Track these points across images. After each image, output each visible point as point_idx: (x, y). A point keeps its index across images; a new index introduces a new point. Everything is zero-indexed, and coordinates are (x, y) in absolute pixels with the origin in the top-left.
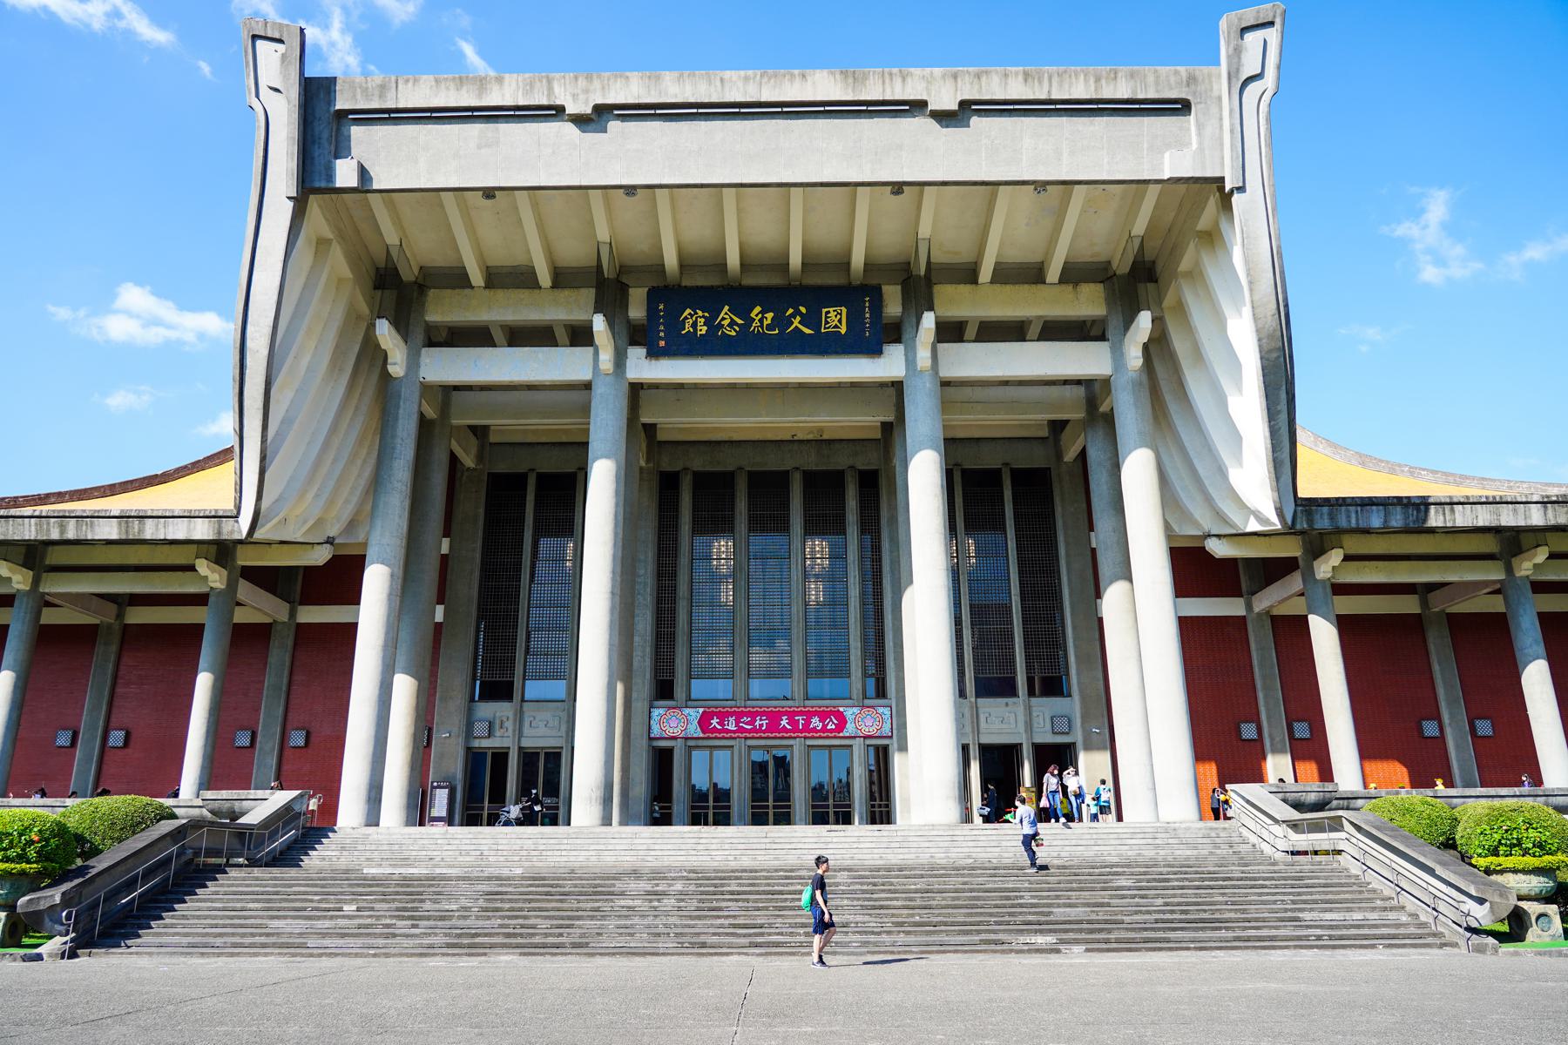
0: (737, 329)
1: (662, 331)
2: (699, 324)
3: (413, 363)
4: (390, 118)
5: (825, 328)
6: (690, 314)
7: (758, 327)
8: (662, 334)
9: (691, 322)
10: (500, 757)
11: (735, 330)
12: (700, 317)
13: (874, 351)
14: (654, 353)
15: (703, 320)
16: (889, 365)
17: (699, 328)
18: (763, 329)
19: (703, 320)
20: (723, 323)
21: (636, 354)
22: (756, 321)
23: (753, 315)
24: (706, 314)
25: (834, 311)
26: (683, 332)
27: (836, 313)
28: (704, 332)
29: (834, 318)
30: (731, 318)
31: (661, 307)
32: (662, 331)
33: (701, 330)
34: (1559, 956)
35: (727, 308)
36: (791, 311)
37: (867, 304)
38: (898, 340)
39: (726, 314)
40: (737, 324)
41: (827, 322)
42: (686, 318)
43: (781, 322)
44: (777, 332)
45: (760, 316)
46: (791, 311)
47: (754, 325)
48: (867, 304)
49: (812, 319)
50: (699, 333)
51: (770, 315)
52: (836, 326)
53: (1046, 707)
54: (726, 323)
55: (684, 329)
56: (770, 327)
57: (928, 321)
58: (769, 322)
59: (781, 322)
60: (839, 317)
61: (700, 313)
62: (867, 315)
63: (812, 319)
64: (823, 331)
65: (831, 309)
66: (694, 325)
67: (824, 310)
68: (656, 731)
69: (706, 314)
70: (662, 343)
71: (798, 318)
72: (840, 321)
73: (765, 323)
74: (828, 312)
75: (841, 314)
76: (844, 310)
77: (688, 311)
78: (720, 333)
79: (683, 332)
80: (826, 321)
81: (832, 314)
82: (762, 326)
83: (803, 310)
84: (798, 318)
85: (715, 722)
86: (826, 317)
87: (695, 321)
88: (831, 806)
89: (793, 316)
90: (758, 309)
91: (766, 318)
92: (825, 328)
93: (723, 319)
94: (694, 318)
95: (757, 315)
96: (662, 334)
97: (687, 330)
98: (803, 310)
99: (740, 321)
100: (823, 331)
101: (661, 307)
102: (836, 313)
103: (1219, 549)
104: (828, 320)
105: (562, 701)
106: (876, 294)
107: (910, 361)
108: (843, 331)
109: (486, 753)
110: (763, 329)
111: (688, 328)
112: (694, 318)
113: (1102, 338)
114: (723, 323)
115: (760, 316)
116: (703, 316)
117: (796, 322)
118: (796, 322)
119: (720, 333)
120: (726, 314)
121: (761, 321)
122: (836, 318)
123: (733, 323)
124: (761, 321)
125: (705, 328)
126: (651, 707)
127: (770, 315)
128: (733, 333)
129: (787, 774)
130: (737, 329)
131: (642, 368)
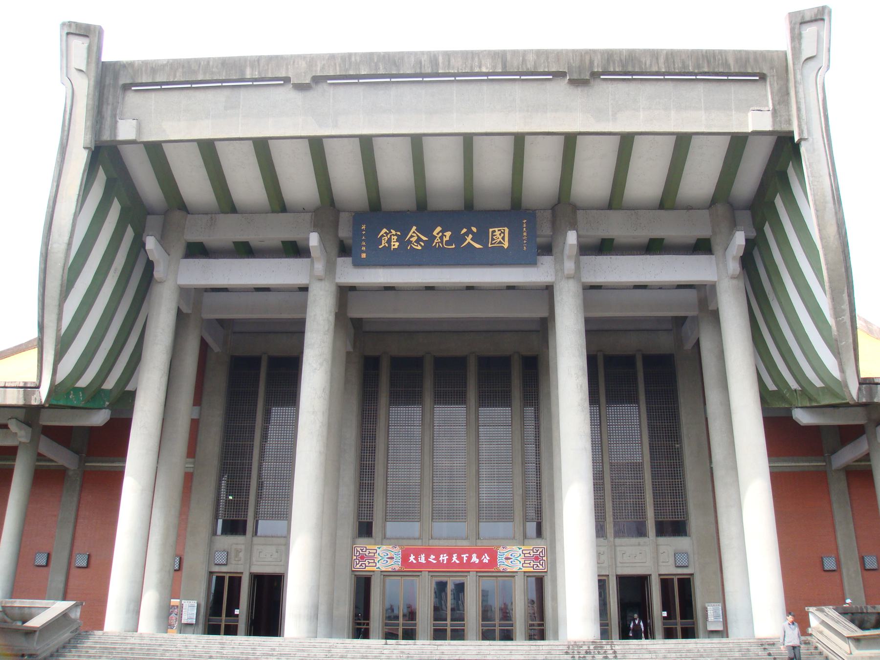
0: (423, 244)
1: (364, 246)
2: (393, 241)
4: (161, 89)
5: (492, 244)
6: (386, 233)
7: (439, 242)
8: (364, 248)
9: (387, 239)
10: (235, 581)
11: (420, 245)
12: (394, 235)
13: (528, 261)
14: (359, 264)
15: (396, 237)
17: (392, 243)
18: (442, 244)
19: (396, 237)
20: (411, 240)
22: (438, 238)
23: (435, 233)
24: (399, 233)
25: (499, 230)
26: (380, 247)
27: (500, 232)
28: (396, 247)
29: (498, 236)
30: (417, 235)
31: (364, 227)
32: (364, 246)
33: (394, 245)
35: (414, 228)
36: (464, 230)
37: (525, 226)
39: (414, 232)
40: (422, 240)
41: (492, 239)
42: (383, 236)
43: (457, 239)
44: (454, 246)
45: (441, 234)
46: (464, 230)
47: (436, 241)
48: (525, 226)
50: (393, 247)
51: (448, 234)
52: (500, 242)
53: (671, 544)
54: (414, 239)
55: (381, 244)
56: (448, 243)
57: (572, 238)
58: (448, 238)
59: (457, 239)
60: (502, 235)
61: (393, 232)
62: (525, 234)
64: (490, 246)
65: (496, 229)
66: (389, 241)
67: (491, 230)
69: (399, 233)
70: (364, 256)
71: (471, 236)
72: (503, 238)
73: (445, 239)
74: (494, 231)
75: (504, 233)
76: (507, 230)
77: (385, 230)
78: (409, 248)
79: (380, 247)
80: (492, 238)
81: (497, 233)
82: (442, 242)
83: (474, 229)
84: (471, 236)
86: (493, 235)
87: (389, 238)
88: (497, 625)
89: (467, 234)
90: (439, 229)
91: (445, 236)
92: (492, 244)
93: (412, 236)
94: (389, 236)
95: (438, 234)
96: (364, 248)
97: (383, 245)
98: (474, 229)
99: (424, 238)
100: (490, 246)
101: (364, 227)
102: (500, 232)
103: (803, 417)
104: (494, 237)
105: (285, 537)
108: (506, 245)
109: (224, 577)
110: (442, 244)
111: (384, 243)
112: (389, 236)
114: (411, 240)
115: (441, 234)
116: (396, 235)
117: (469, 239)
118: (469, 239)
119: (409, 248)
120: (414, 232)
121: (441, 238)
122: (500, 236)
123: (419, 240)
124: (441, 238)
125: (397, 244)
126: (354, 543)
127: (448, 234)
128: (419, 248)
130: (423, 244)
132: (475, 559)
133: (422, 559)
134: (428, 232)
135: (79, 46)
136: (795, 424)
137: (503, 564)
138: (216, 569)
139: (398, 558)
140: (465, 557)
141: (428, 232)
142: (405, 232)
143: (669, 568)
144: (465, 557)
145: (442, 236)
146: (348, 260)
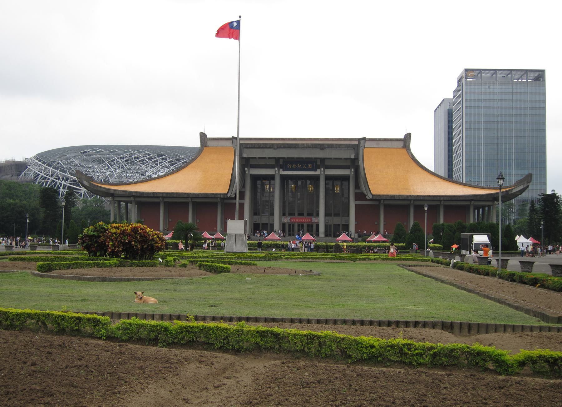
3: (249, 171)
13: (315, 170)
14: (284, 170)
16: (317, 173)
21: (281, 170)
38: (319, 168)
43: (302, 166)
49: (307, 166)
59: (302, 166)
68: (283, 221)
85: (292, 220)
87: (290, 166)
106: (316, 162)
107: (321, 173)
122: (310, 166)
131: (282, 172)
138: (255, 222)
142: (292, 165)
143: (344, 223)
145: (299, 166)
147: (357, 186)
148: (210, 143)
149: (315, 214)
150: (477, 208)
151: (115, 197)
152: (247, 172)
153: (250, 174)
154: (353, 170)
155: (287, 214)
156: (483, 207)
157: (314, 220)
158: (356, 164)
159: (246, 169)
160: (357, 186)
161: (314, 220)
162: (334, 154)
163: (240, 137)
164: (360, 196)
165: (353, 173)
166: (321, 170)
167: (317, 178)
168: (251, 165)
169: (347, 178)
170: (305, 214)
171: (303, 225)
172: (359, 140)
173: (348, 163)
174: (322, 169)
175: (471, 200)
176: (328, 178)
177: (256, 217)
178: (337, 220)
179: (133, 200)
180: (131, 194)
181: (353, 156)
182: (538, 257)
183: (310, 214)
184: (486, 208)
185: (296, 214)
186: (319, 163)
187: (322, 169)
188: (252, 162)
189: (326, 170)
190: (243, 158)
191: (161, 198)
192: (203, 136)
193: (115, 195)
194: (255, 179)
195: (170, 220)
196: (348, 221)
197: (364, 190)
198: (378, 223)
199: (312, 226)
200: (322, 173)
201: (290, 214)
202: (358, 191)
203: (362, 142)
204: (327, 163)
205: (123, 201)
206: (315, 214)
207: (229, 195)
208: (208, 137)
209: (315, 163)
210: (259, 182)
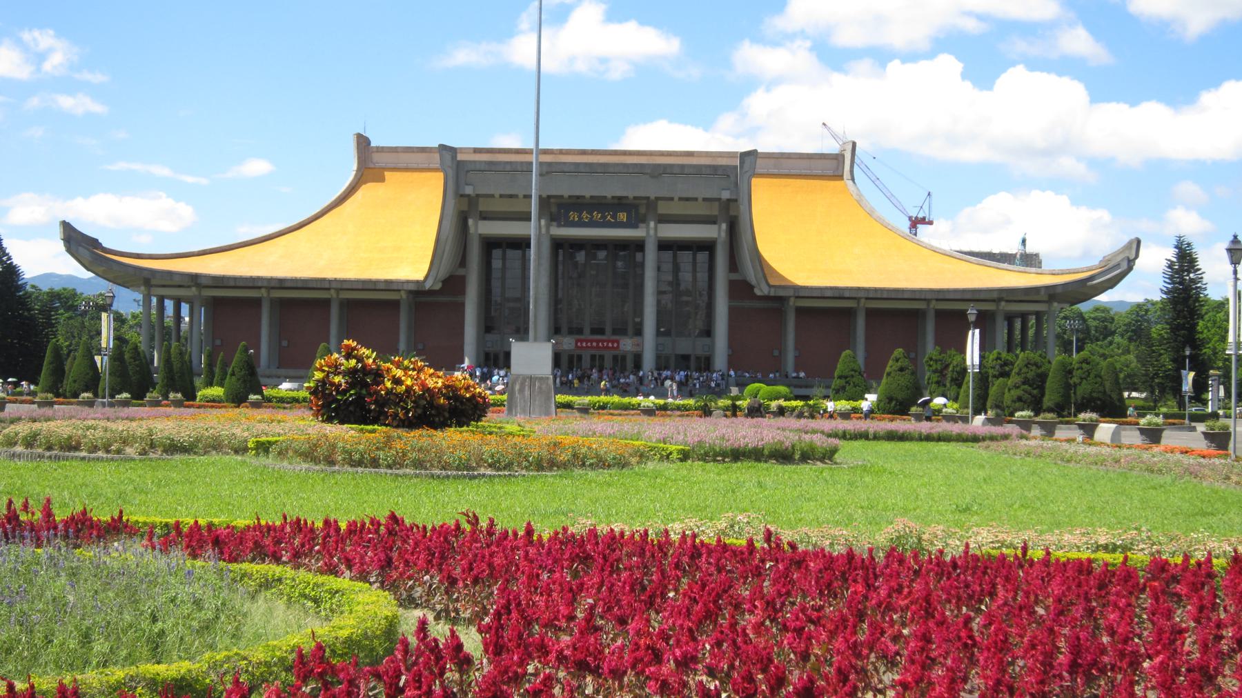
13: (635, 226)
14: (559, 226)
34: (734, 415)
43: (604, 217)
49: (614, 217)
51: (600, 215)
59: (604, 217)
63: (614, 217)
87: (574, 216)
106: (636, 207)
107: (648, 232)
108: (625, 220)
111: (571, 218)
113: (714, 223)
122: (623, 216)
123: (587, 217)
129: (603, 360)
132: (610, 345)
133: (584, 344)
134: (591, 215)
135: (448, 156)
136: (754, 294)
137: (622, 347)
138: (487, 349)
139: (574, 344)
140: (605, 344)
141: (591, 215)
142: (581, 214)
143: (699, 352)
144: (605, 344)
145: (597, 216)
146: (555, 223)
147: (734, 265)
148: (376, 157)
149: (630, 330)
150: (1010, 318)
151: (152, 286)
152: (472, 230)
153: (480, 235)
154: (724, 226)
155: (564, 329)
156: (1024, 316)
157: (627, 344)
158: (732, 213)
159: (471, 222)
160: (734, 265)
161: (627, 344)
162: (683, 188)
163: (541, 146)
164: (741, 289)
165: (723, 234)
166: (648, 227)
167: (639, 245)
168: (481, 212)
169: (707, 246)
170: (608, 330)
171: (602, 357)
172: (745, 155)
173: (714, 210)
174: (652, 224)
175: (999, 300)
176: (665, 246)
177: (489, 337)
178: (683, 346)
179: (196, 293)
180: (195, 279)
181: (726, 195)
182: (1195, 438)
183: (621, 331)
184: (1032, 321)
185: (587, 330)
186: (642, 210)
187: (652, 224)
188: (483, 206)
189: (661, 226)
190: (462, 196)
191: (263, 291)
192: (363, 142)
193: (153, 282)
194: (491, 244)
195: (285, 343)
196: (712, 347)
197: (751, 276)
198: (780, 353)
199: (624, 358)
200: (652, 232)
201: (571, 331)
202: (735, 277)
203: (748, 160)
204: (663, 209)
205: (170, 298)
206: (630, 330)
207: (428, 286)
208: (373, 144)
209: (636, 210)
210: (497, 253)
